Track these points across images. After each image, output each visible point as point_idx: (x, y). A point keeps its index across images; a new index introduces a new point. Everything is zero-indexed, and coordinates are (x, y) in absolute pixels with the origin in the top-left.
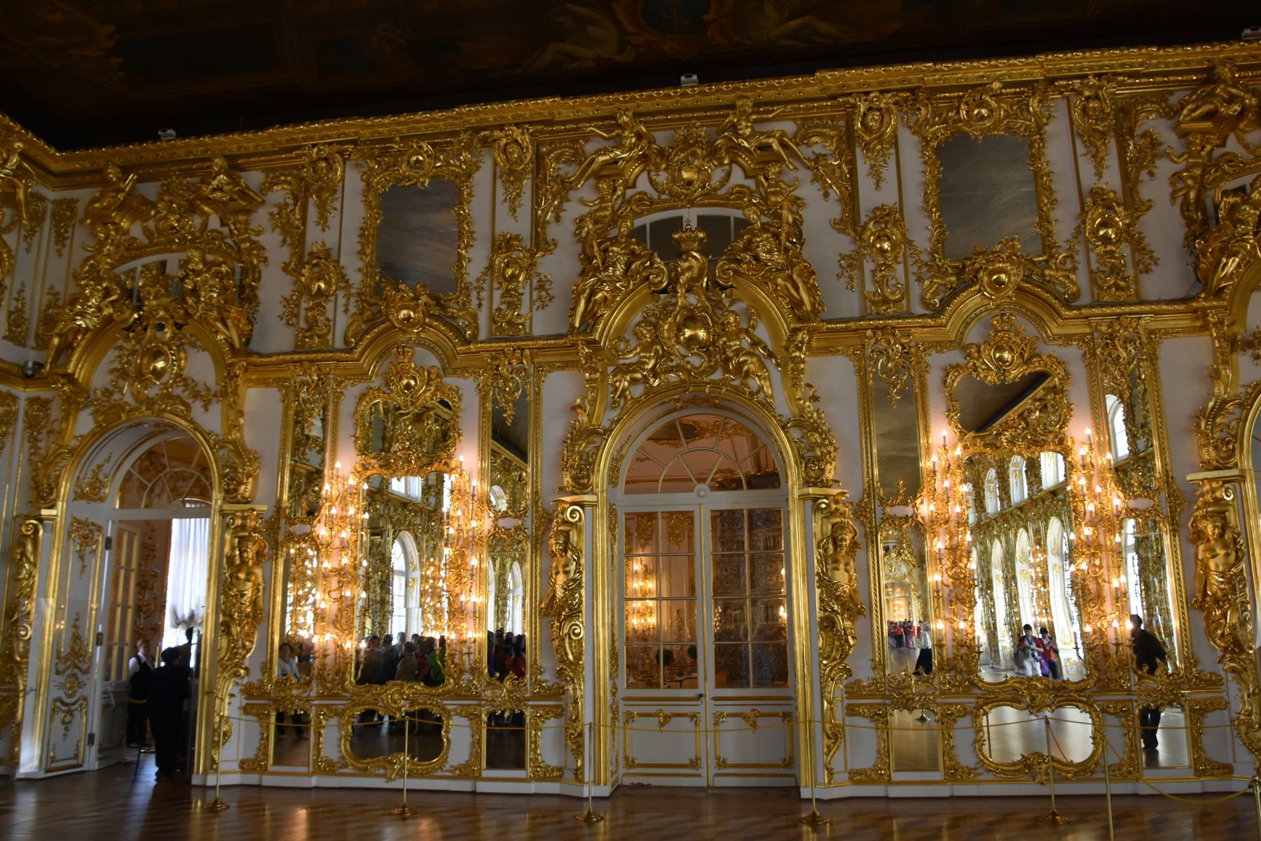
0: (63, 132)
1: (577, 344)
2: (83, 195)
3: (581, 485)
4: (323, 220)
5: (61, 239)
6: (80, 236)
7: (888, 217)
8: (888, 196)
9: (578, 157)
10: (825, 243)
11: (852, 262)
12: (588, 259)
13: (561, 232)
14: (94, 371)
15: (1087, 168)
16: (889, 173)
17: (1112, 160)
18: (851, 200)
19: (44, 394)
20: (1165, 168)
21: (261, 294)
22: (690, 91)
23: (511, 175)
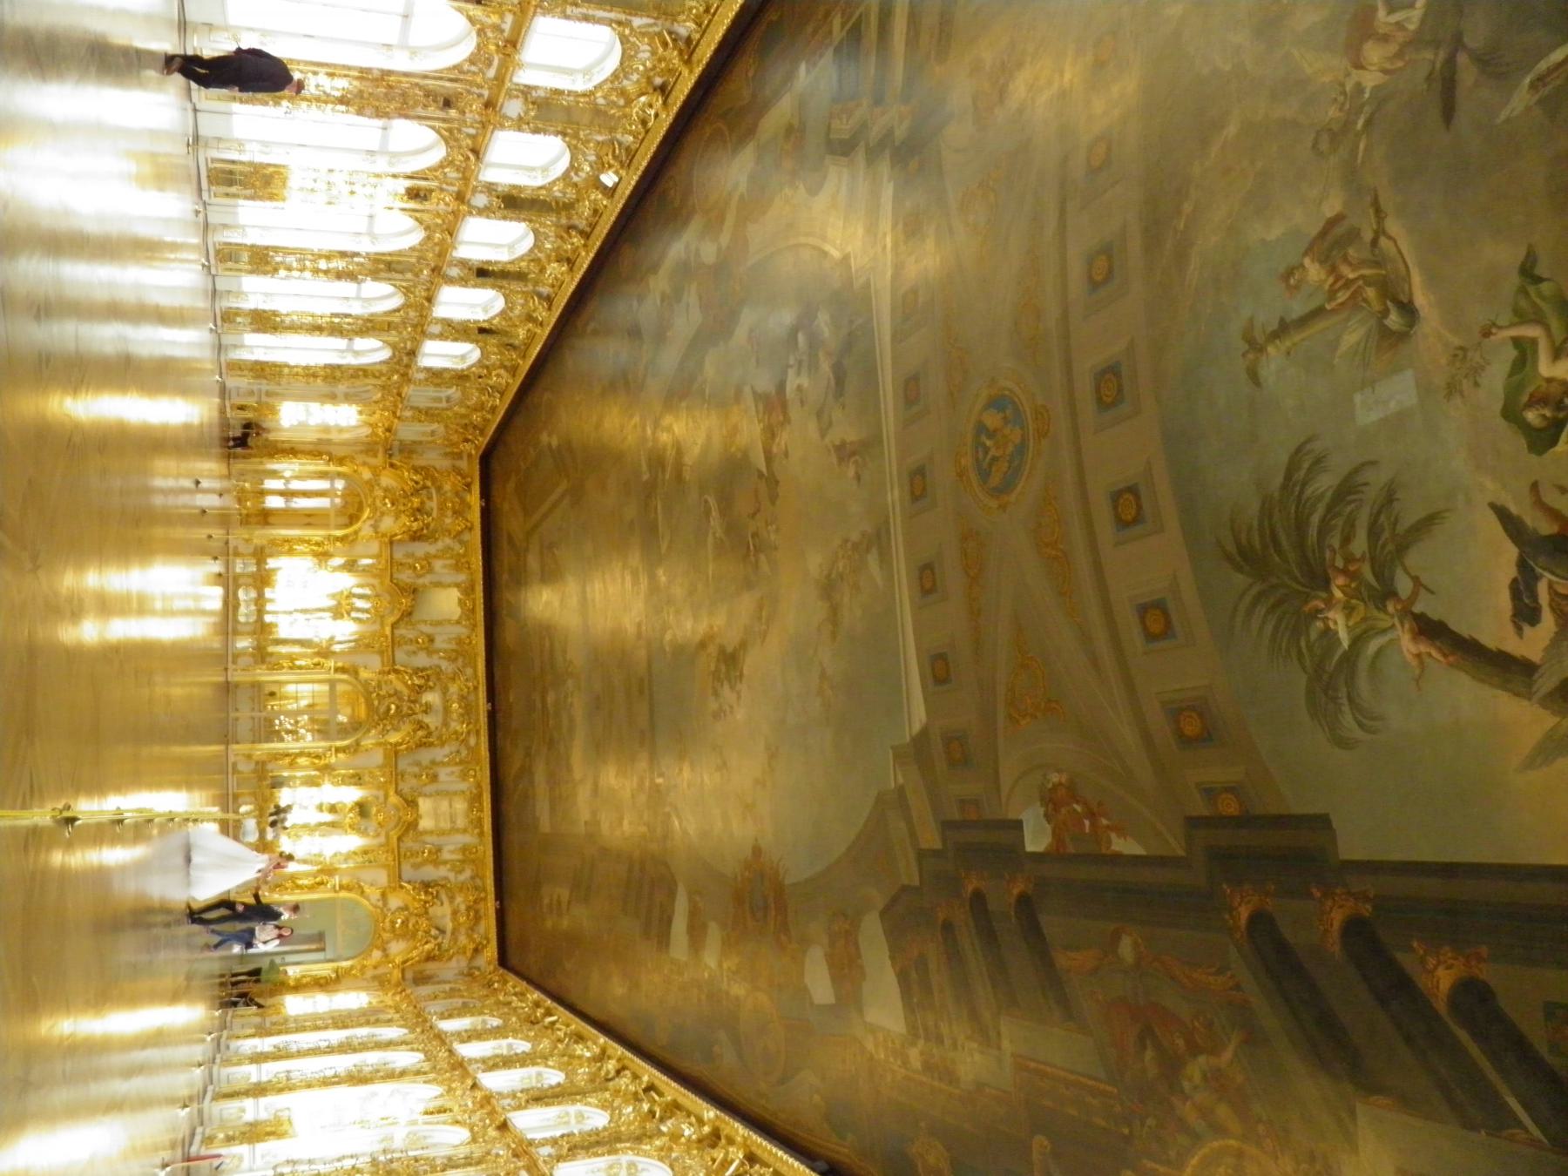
0: (486, 459)
4: (445, 566)
5: (446, 454)
6: (445, 464)
7: (434, 778)
10: (425, 756)
11: (418, 764)
12: (422, 670)
13: (435, 660)
14: (387, 480)
15: (451, 847)
16: (453, 778)
19: (380, 455)
20: (451, 876)
21: (417, 544)
22: (483, 706)
23: (459, 641)
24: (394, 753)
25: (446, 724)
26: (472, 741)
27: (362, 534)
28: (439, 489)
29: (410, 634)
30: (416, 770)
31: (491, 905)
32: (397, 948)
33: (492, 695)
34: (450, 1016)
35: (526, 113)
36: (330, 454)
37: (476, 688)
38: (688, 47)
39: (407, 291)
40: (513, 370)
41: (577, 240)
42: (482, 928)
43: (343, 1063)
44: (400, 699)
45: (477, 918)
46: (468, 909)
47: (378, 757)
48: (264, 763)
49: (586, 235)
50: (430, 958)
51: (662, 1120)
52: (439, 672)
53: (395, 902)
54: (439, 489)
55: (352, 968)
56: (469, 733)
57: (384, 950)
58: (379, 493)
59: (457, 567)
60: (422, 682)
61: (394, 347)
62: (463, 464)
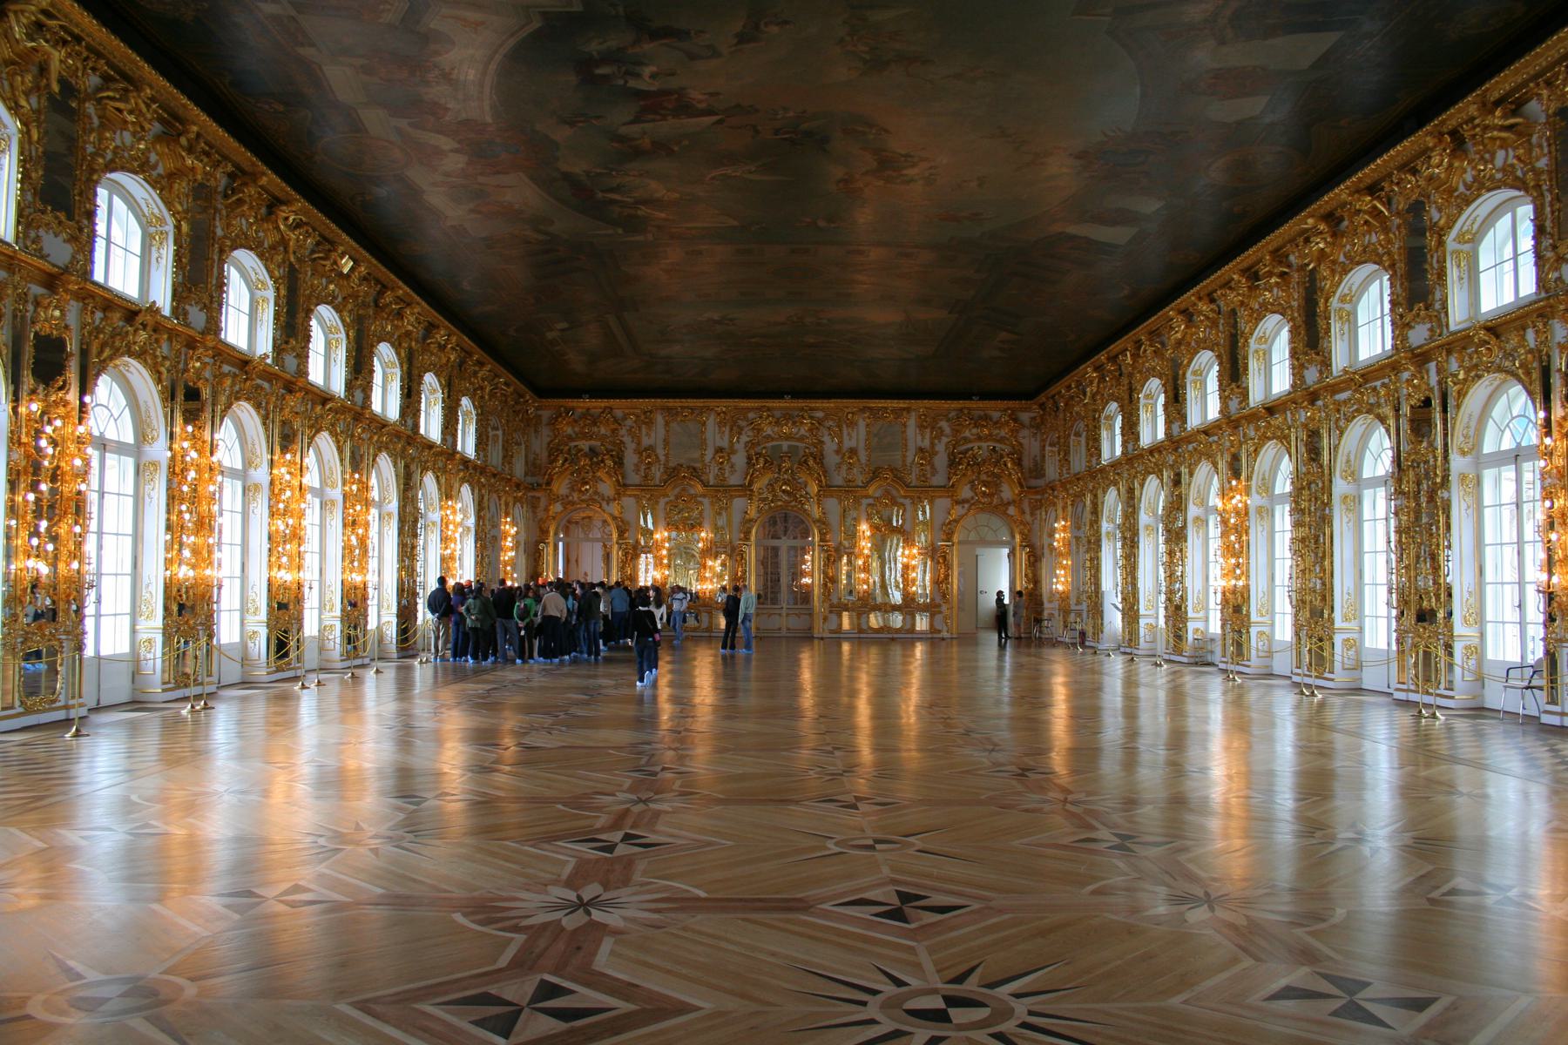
0: (543, 392)
1: (746, 490)
2: (546, 414)
3: (747, 538)
4: (648, 435)
5: (536, 431)
6: (546, 432)
7: (853, 452)
8: (853, 444)
9: (746, 419)
10: (832, 459)
11: (839, 466)
12: (749, 458)
13: (740, 447)
14: (561, 487)
16: (854, 435)
17: (928, 436)
18: (840, 442)
19: (537, 494)
20: (945, 440)
22: (786, 403)
23: (721, 424)
24: (826, 489)
25: (801, 439)
26: (820, 414)
27: (616, 513)
28: (570, 438)
29: (714, 470)
30: (844, 467)
31: (976, 405)
32: (1008, 492)
33: (778, 395)
34: (1099, 450)
35: (293, 349)
36: (537, 543)
37: (769, 409)
38: (239, 175)
39: (425, 469)
40: (481, 364)
41: (388, 297)
42: (996, 415)
43: (1151, 549)
44: (777, 480)
45: (987, 418)
46: (976, 426)
47: (832, 504)
48: (832, 606)
49: (385, 288)
50: (1019, 463)
51: (1289, 266)
52: (750, 445)
53: (965, 492)
54: (570, 438)
55: (1021, 533)
56: (812, 418)
57: (1009, 503)
58: (576, 495)
59: (650, 423)
60: (762, 460)
61: (463, 481)
62: (546, 414)
